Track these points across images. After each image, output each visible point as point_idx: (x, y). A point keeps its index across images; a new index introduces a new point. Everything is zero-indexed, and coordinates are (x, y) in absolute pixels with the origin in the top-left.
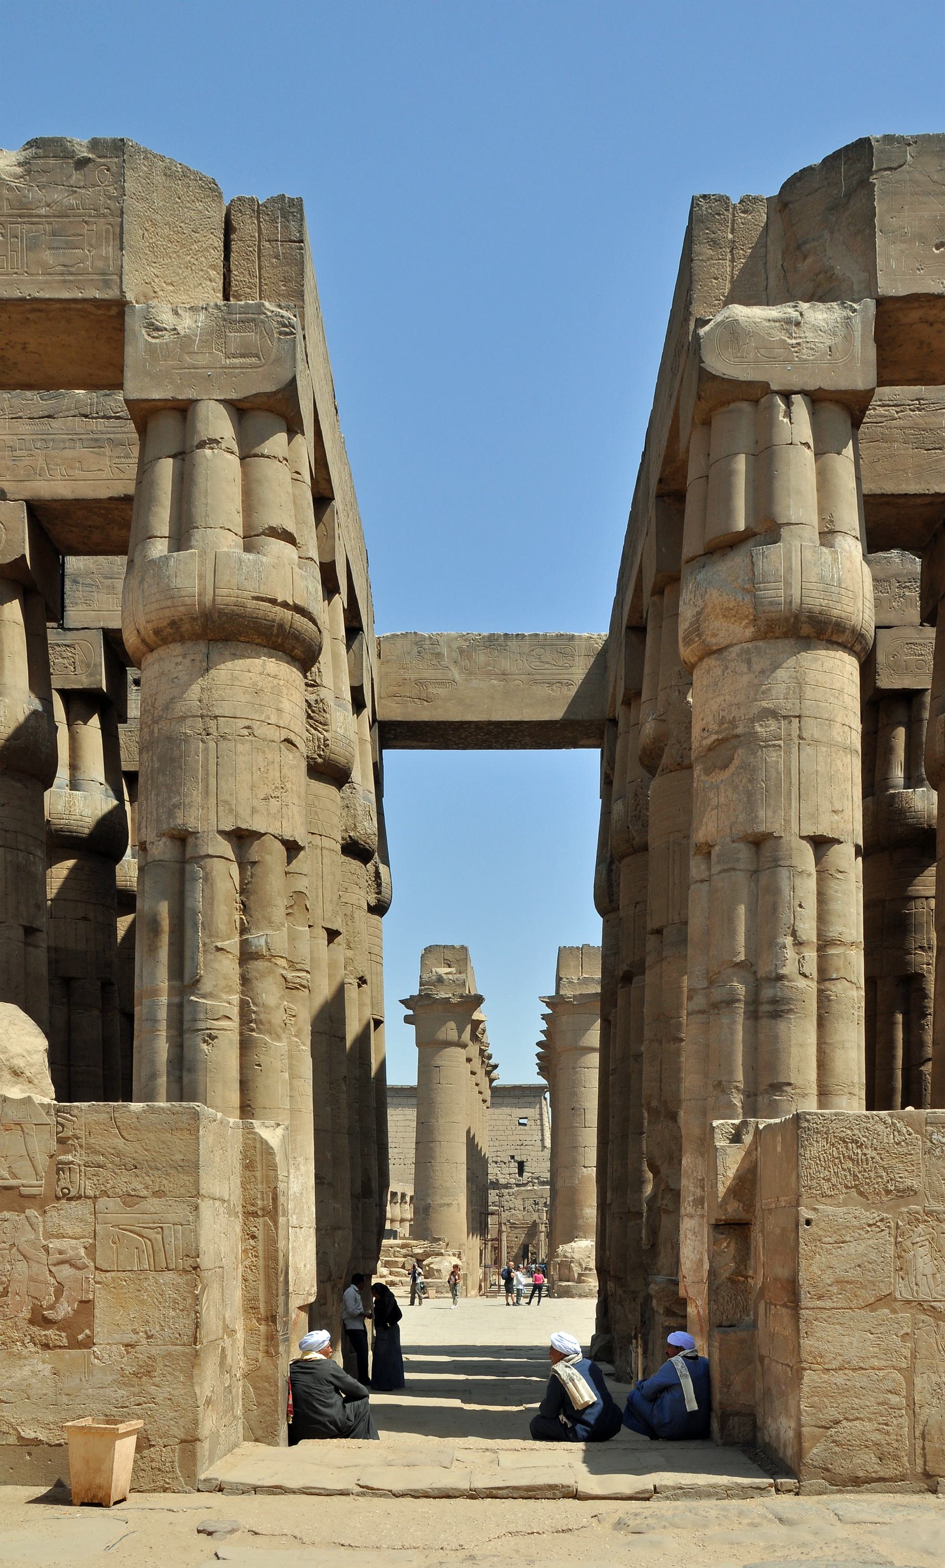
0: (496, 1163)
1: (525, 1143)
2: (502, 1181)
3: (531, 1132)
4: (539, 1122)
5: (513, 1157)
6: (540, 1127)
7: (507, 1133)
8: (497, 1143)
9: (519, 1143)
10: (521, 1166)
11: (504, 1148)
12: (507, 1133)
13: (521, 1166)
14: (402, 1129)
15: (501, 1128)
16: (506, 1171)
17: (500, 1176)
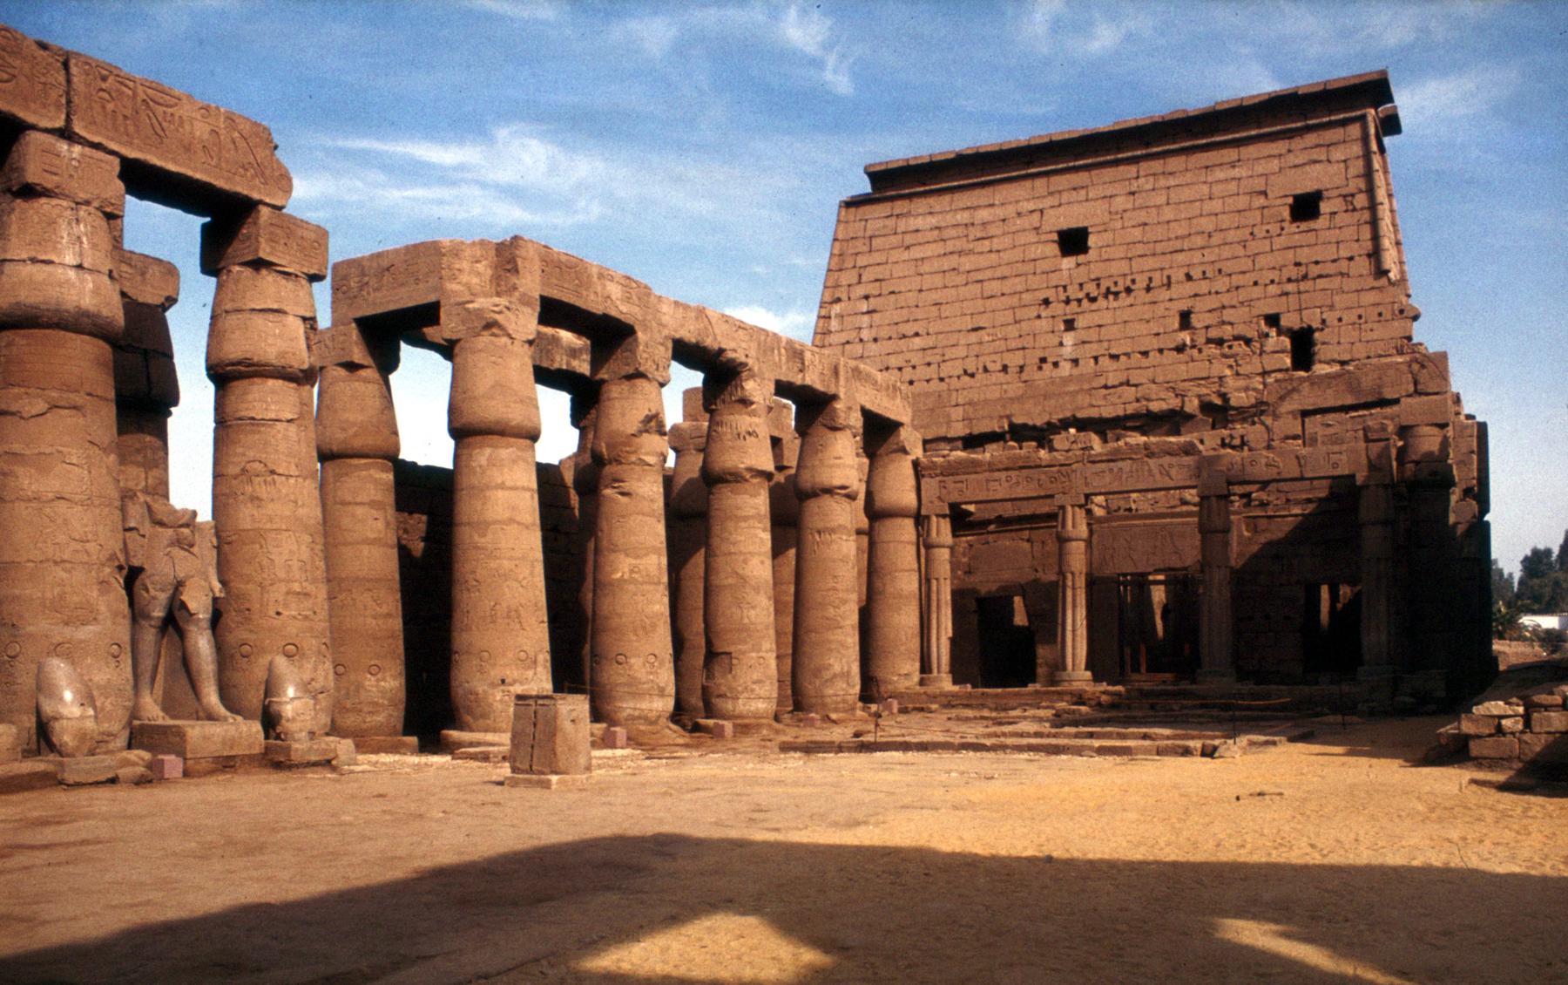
0: (1220, 342)
1: (1315, 270)
2: (1239, 399)
3: (1334, 235)
4: (1361, 200)
5: (1273, 320)
6: (1366, 216)
7: (1254, 247)
8: (1222, 284)
9: (1294, 272)
10: (1303, 346)
11: (1243, 295)
12: (1254, 247)
13: (1303, 346)
14: (938, 280)
15: (1232, 236)
16: (1253, 365)
17: (1231, 383)
